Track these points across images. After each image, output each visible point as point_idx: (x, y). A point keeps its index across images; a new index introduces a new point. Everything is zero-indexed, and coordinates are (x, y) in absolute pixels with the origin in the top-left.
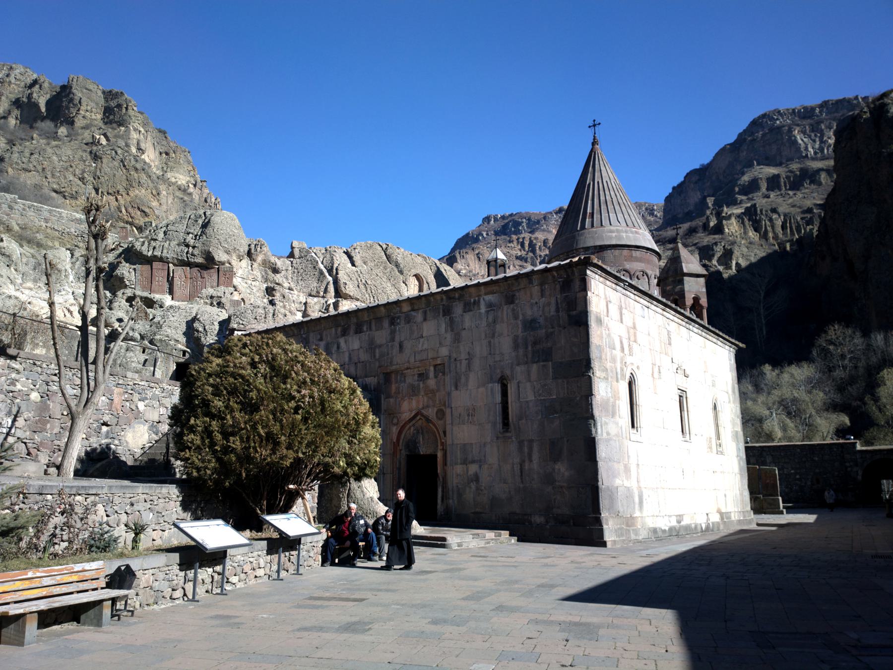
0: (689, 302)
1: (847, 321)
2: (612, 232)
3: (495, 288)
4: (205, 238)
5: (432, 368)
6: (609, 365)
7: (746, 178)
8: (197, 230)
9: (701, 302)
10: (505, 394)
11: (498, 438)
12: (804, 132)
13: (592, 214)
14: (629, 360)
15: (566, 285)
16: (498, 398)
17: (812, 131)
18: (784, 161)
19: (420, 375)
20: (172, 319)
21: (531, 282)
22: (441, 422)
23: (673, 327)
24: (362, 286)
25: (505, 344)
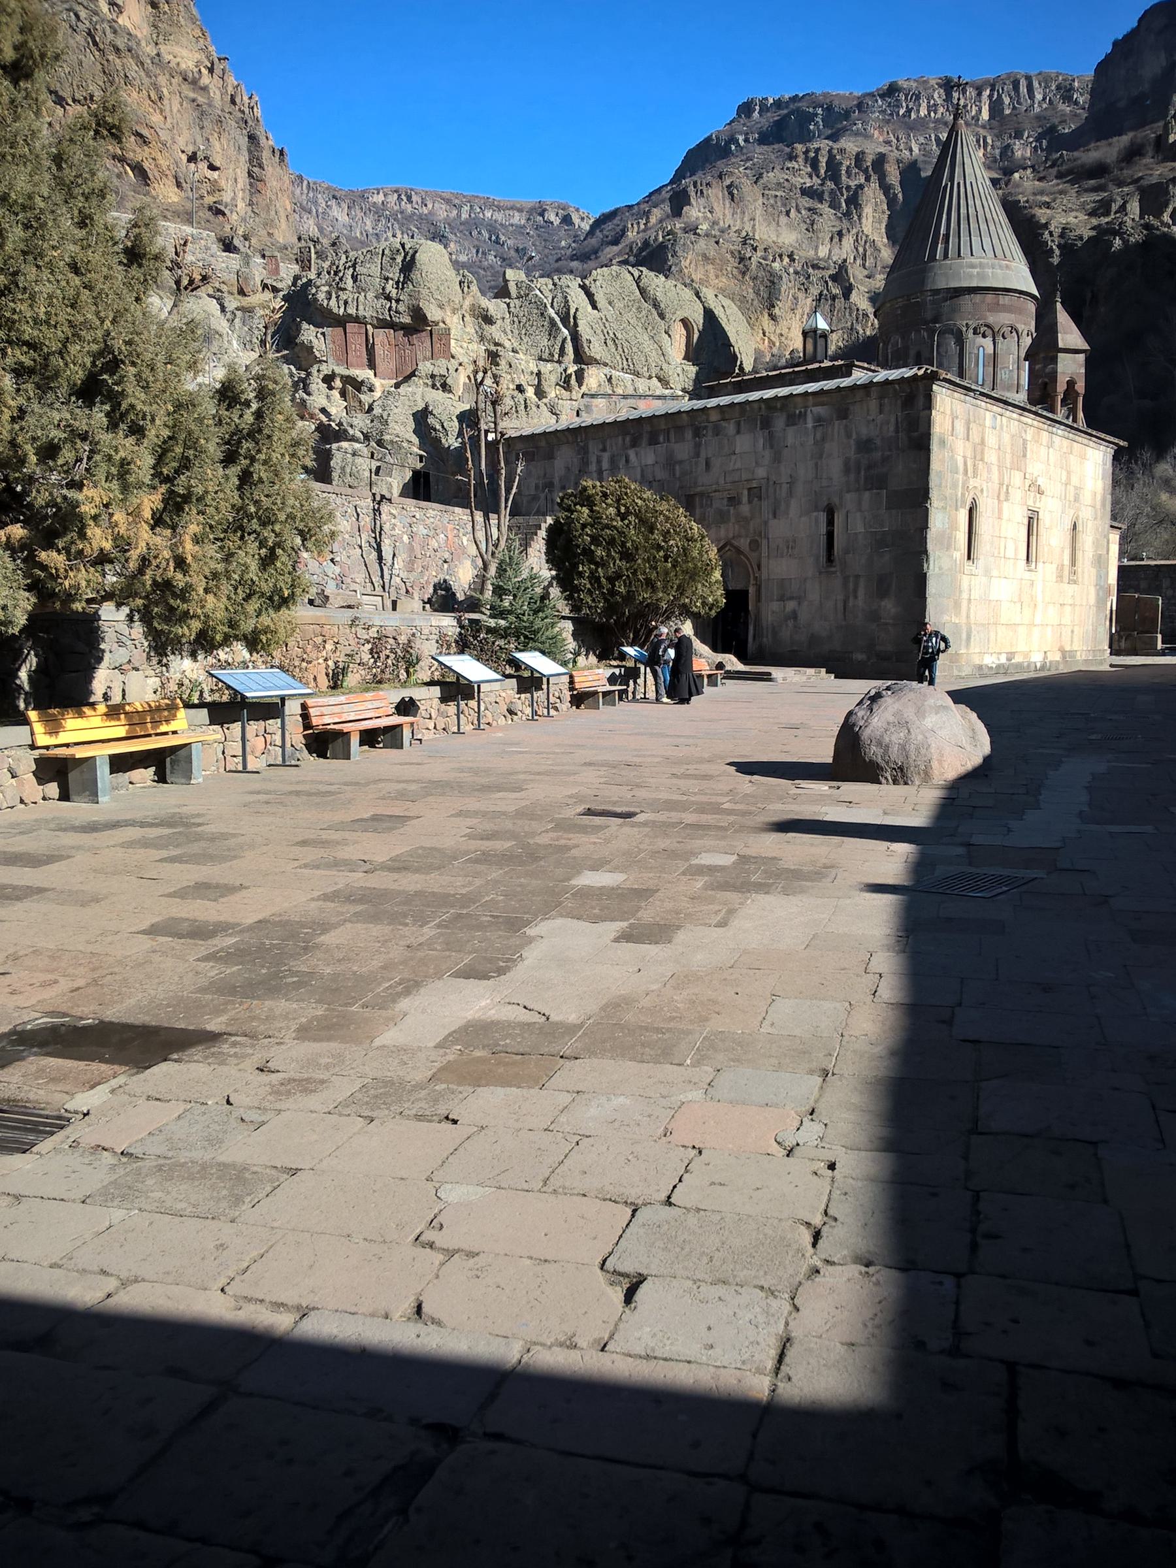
0: (1061, 387)
2: (973, 266)
3: (825, 399)
5: (746, 492)
6: (948, 492)
8: (395, 273)
9: (1076, 387)
10: (830, 522)
11: (820, 573)
13: (947, 236)
14: (972, 483)
16: (823, 530)
19: (730, 499)
20: (396, 411)
21: (868, 395)
22: (755, 554)
23: (1029, 434)
24: (609, 342)
25: (834, 467)
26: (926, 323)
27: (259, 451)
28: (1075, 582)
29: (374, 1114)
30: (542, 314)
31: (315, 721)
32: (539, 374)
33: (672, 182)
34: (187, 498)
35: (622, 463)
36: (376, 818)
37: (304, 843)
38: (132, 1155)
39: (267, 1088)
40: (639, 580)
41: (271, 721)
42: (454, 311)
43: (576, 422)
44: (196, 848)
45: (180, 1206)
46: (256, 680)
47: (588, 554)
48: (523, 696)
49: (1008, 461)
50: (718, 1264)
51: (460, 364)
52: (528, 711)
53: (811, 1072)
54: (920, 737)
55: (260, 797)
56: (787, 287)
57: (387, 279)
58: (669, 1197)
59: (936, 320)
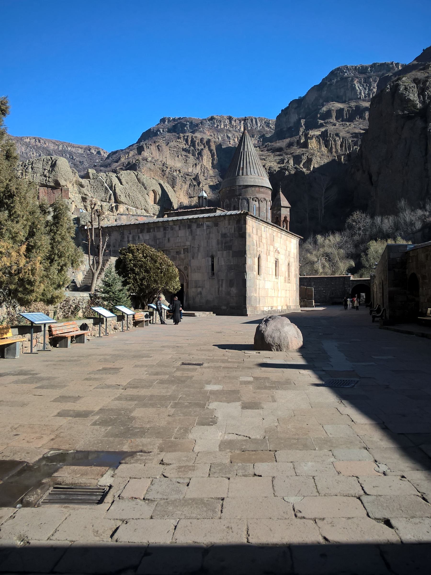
0: (282, 219)
1: (364, 209)
2: (251, 178)
3: (210, 219)
4: (54, 173)
5: (182, 250)
6: (252, 252)
7: (324, 109)
8: (48, 168)
10: (213, 261)
12: (360, 83)
13: (243, 168)
14: (259, 249)
15: (238, 221)
17: (365, 82)
18: (347, 100)
21: (225, 219)
22: (186, 272)
23: (275, 233)
24: (127, 196)
25: (214, 242)
26: (237, 196)
27: (57, 231)
28: (290, 283)
29: (228, 476)
30: (102, 185)
31: (54, 333)
32: (101, 206)
33: (137, 143)
34: (33, 247)
35: (137, 238)
36: (104, 369)
37: (87, 379)
38: (149, 500)
39: (175, 470)
40: (152, 280)
41: (38, 333)
42: (70, 182)
43: (115, 224)
44: (45, 383)
45: (194, 515)
46: (37, 317)
47: (133, 270)
48: (119, 322)
49: (269, 242)
50: (406, 511)
51: (73, 201)
52: (120, 328)
53: (360, 448)
54: (284, 334)
55: (50, 363)
56: (179, 181)
57: (45, 169)
58: (365, 492)
59: (240, 195)
